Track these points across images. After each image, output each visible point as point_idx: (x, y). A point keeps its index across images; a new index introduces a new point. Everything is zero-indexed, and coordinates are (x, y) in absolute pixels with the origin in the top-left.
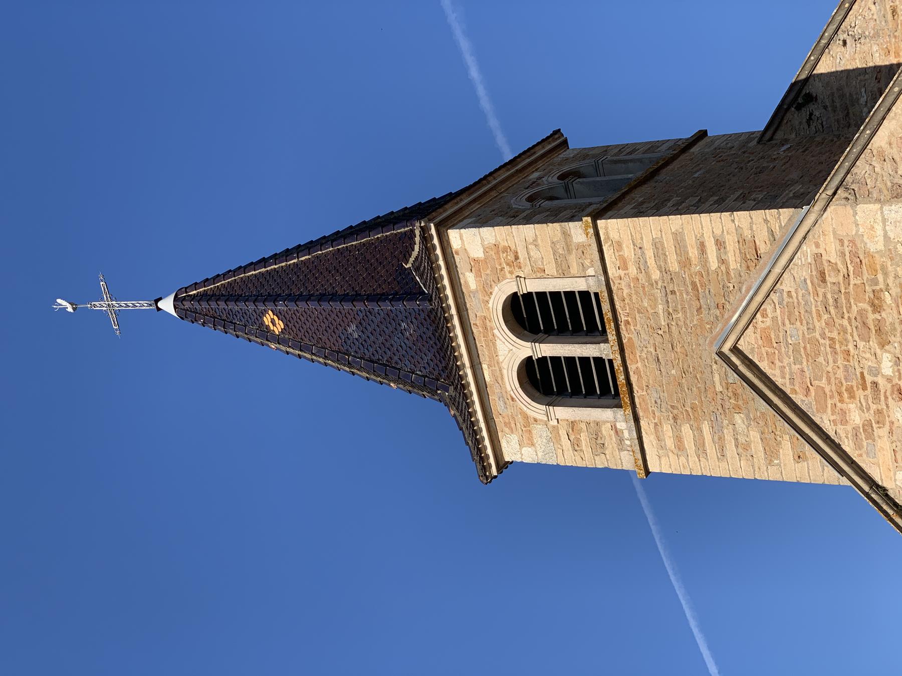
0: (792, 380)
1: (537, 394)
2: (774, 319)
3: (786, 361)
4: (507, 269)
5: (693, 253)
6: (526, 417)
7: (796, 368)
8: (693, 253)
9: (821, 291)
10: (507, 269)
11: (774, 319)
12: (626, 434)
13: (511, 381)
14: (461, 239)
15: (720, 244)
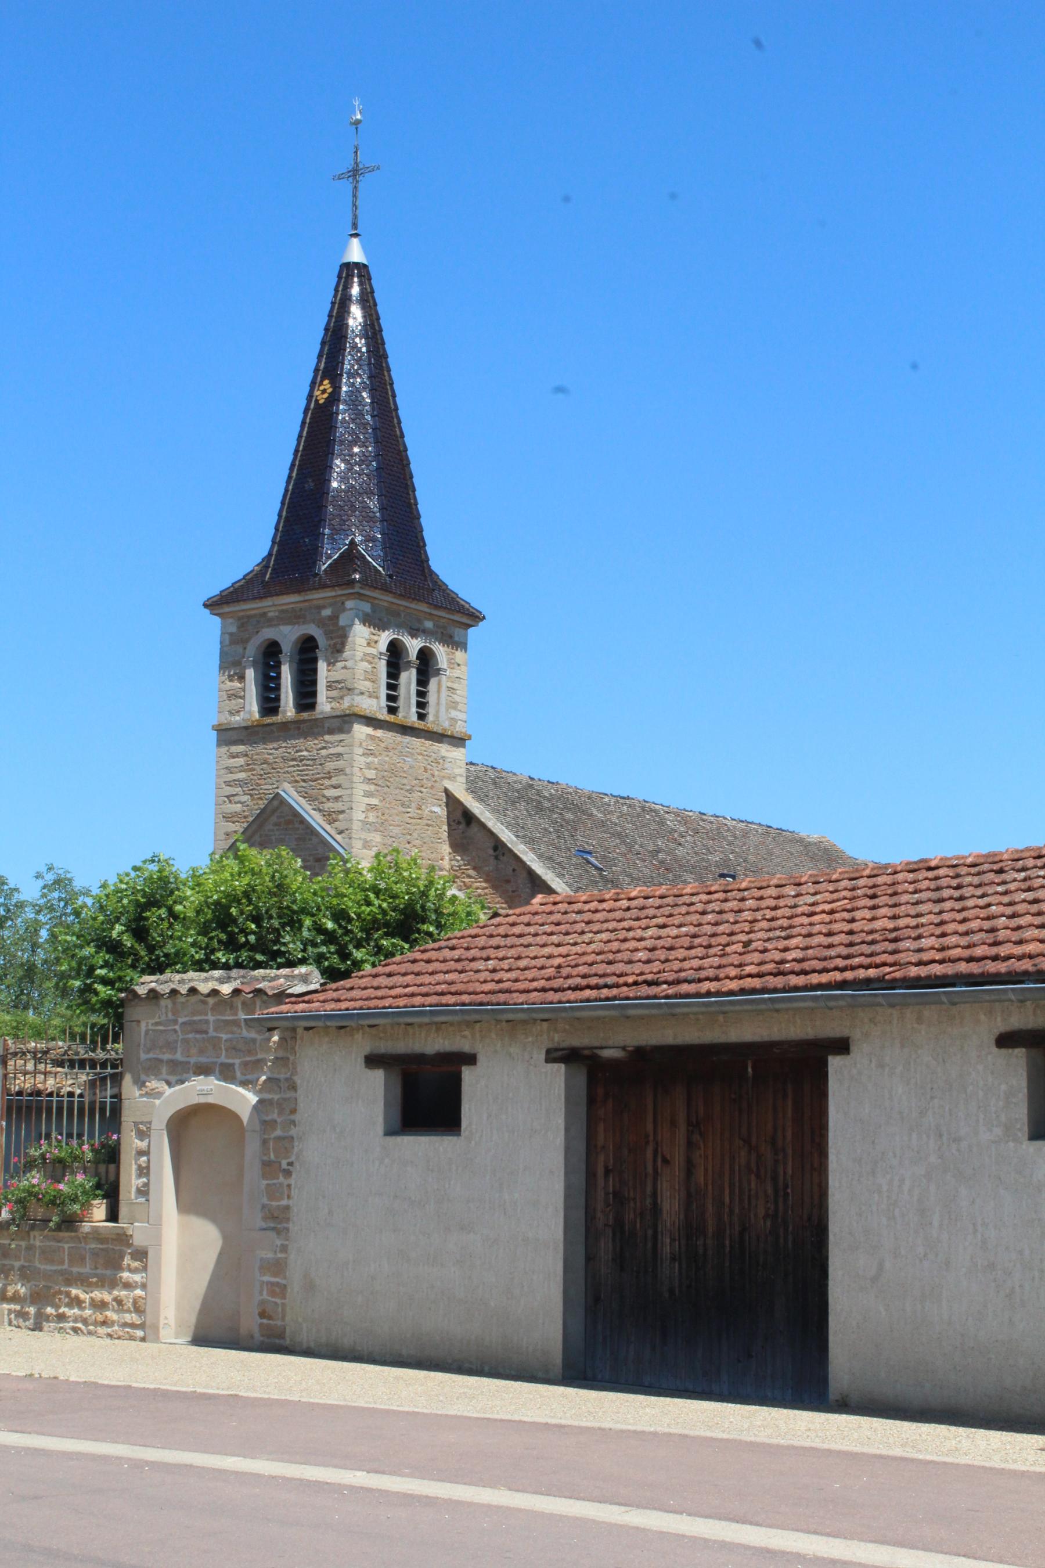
0: (267, 835)
1: (263, 649)
2: (298, 829)
3: (277, 833)
4: (332, 642)
5: (334, 781)
6: (247, 641)
7: (273, 838)
8: (334, 781)
9: (311, 858)
10: (332, 642)
11: (298, 829)
12: (237, 718)
13: (269, 633)
14: (351, 609)
15: (337, 799)
